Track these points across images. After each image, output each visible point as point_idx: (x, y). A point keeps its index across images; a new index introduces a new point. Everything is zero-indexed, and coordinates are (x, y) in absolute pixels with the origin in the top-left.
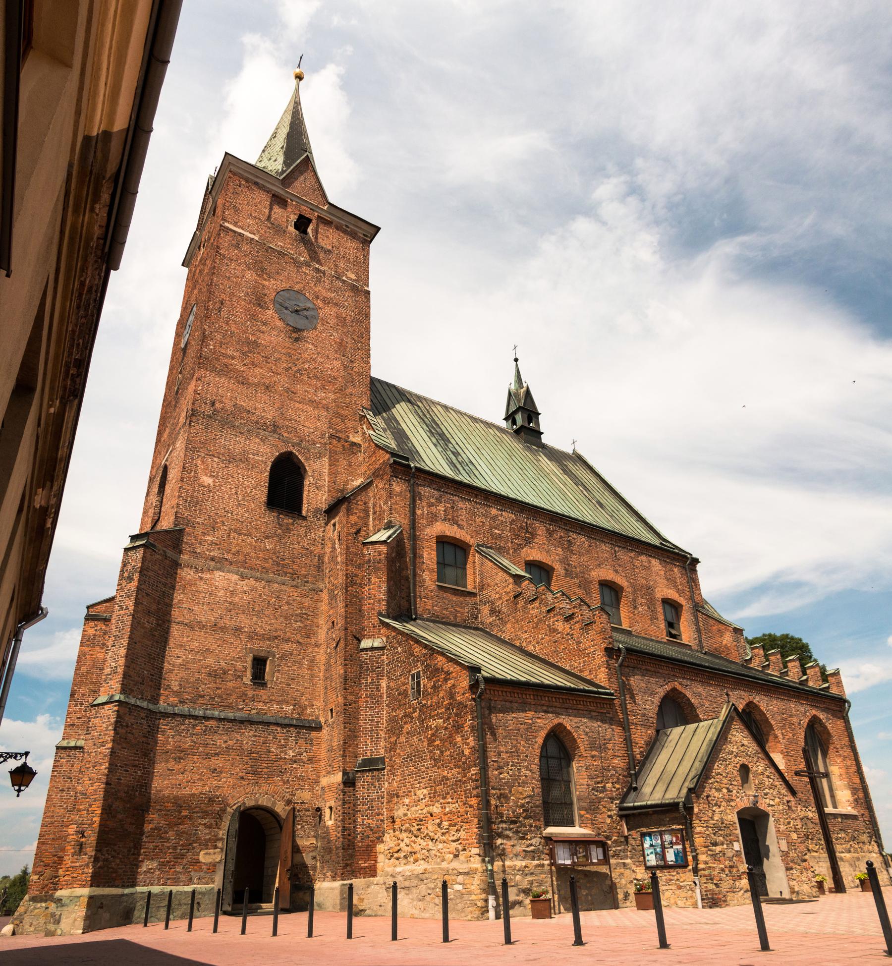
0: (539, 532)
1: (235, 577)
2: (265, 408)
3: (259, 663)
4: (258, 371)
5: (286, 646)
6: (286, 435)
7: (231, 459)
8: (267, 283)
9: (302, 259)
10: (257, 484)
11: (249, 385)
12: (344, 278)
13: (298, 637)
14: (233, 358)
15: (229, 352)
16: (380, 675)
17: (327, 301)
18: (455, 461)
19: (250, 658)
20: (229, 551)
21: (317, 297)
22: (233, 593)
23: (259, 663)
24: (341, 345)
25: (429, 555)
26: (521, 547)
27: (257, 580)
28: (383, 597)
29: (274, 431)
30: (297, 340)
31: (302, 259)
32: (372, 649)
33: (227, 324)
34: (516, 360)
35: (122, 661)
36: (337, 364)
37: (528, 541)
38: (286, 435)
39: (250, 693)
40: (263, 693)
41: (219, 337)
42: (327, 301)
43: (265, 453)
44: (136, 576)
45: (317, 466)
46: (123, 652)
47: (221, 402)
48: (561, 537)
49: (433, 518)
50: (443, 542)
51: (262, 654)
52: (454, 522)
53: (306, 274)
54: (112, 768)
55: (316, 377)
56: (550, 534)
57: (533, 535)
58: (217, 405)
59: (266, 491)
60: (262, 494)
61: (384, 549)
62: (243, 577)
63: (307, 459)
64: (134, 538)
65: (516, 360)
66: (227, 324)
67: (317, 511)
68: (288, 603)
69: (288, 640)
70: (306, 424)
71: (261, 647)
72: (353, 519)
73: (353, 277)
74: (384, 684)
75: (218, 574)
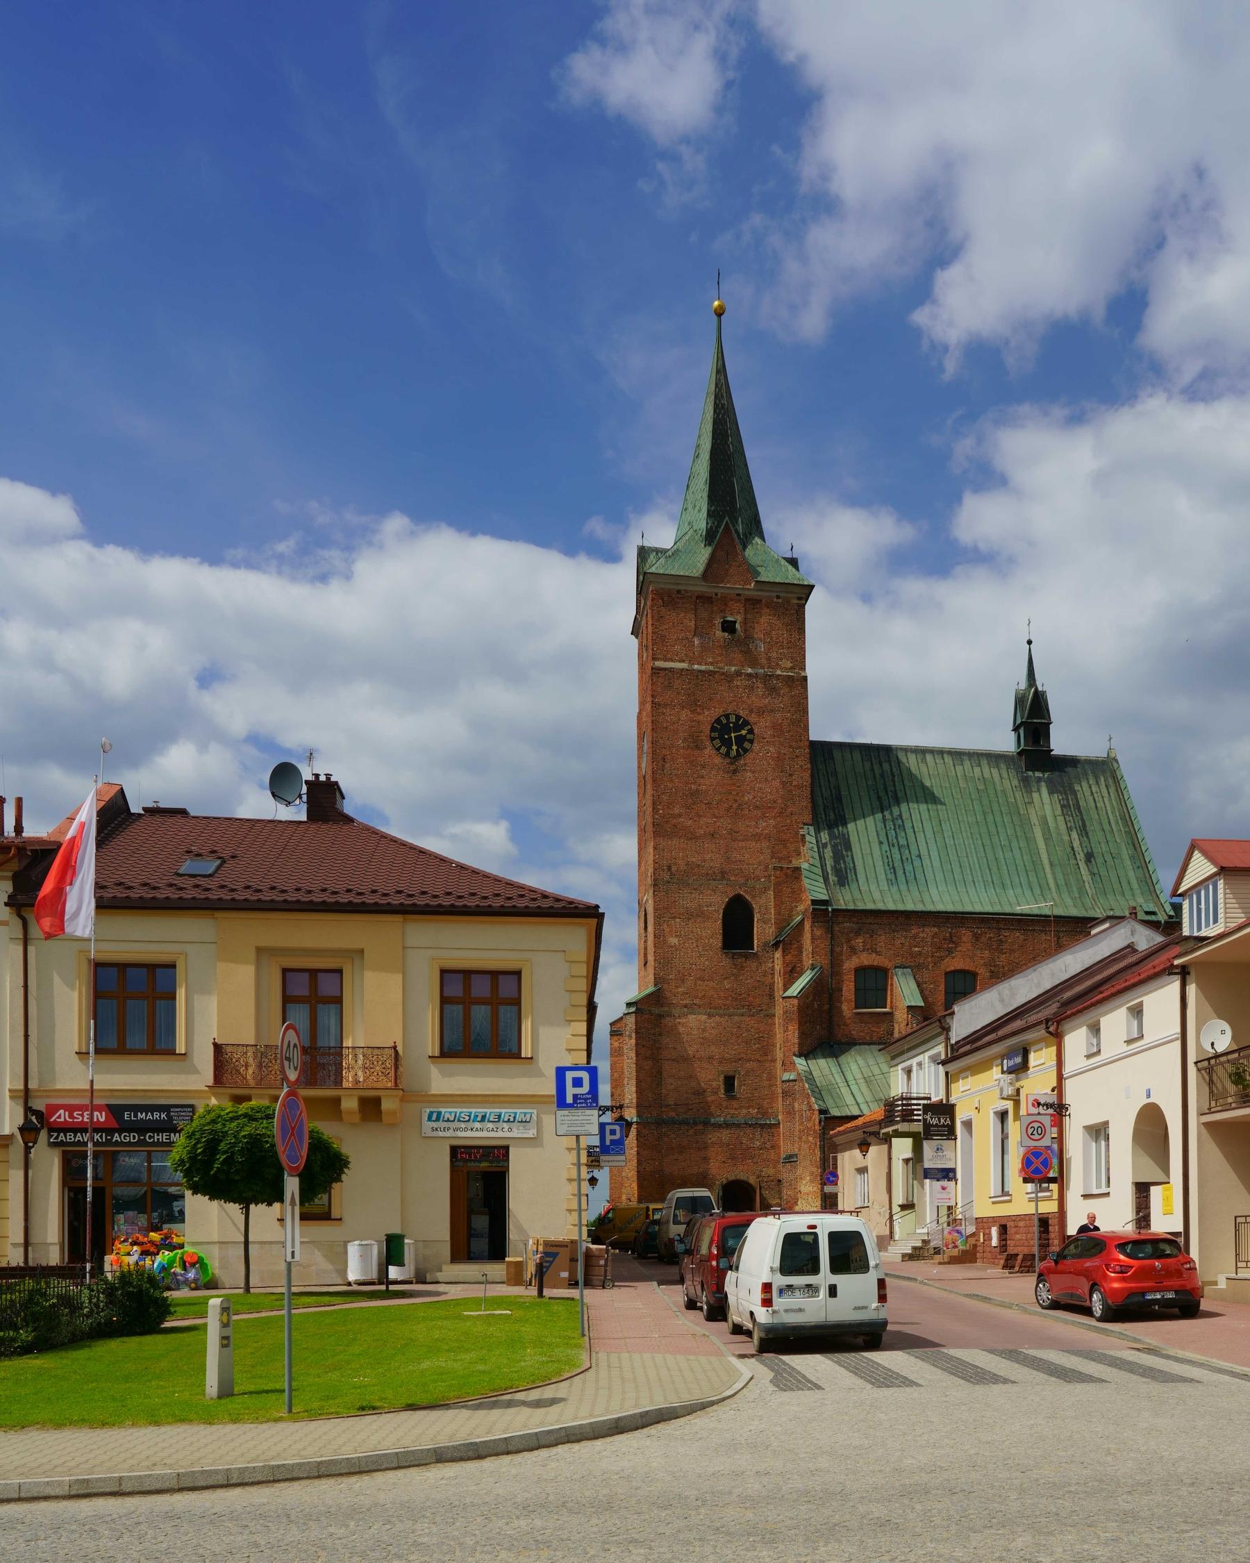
0: (964, 939)
1: (704, 1017)
2: (712, 857)
3: (729, 1082)
4: (703, 821)
5: (749, 1065)
6: (733, 878)
7: (690, 916)
8: (701, 717)
9: (733, 669)
10: (713, 931)
11: (697, 838)
12: (779, 672)
13: (758, 1056)
14: (680, 815)
15: (677, 811)
16: (794, 1099)
17: (761, 712)
18: (898, 864)
19: (722, 1078)
20: (697, 997)
21: (751, 711)
22: (704, 1030)
23: (729, 1082)
24: (779, 759)
25: (848, 989)
26: (942, 959)
27: (721, 1016)
28: (796, 1041)
29: (723, 878)
30: (735, 772)
31: (733, 669)
32: (789, 1081)
33: (672, 781)
34: (1030, 642)
35: (634, 1095)
36: (777, 783)
37: (950, 951)
38: (733, 878)
39: (724, 1104)
40: (735, 1104)
41: (665, 798)
42: (761, 712)
43: (716, 902)
44: (634, 1035)
45: (763, 901)
46: (634, 1089)
47: (675, 864)
48: (990, 938)
49: (853, 950)
50: (861, 971)
51: (731, 1074)
52: (874, 950)
53: (738, 687)
54: (639, 1162)
55: (757, 807)
56: (977, 937)
57: (957, 944)
58: (674, 869)
59: (721, 937)
60: (718, 942)
61: (796, 1002)
62: (710, 1016)
63: (754, 897)
64: (629, 1005)
65: (1030, 642)
66: (672, 781)
67: (766, 944)
68: (747, 1030)
69: (749, 1060)
70: (751, 861)
71: (728, 1069)
72: (789, 958)
73: (789, 665)
74: (796, 1105)
75: (691, 1017)
